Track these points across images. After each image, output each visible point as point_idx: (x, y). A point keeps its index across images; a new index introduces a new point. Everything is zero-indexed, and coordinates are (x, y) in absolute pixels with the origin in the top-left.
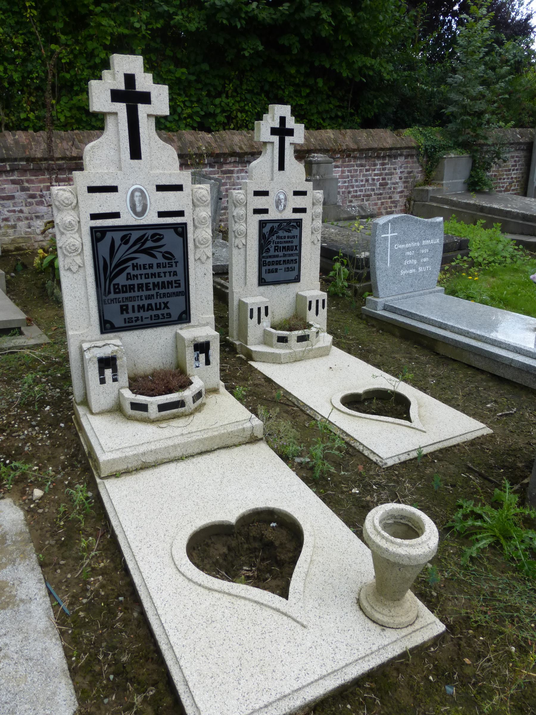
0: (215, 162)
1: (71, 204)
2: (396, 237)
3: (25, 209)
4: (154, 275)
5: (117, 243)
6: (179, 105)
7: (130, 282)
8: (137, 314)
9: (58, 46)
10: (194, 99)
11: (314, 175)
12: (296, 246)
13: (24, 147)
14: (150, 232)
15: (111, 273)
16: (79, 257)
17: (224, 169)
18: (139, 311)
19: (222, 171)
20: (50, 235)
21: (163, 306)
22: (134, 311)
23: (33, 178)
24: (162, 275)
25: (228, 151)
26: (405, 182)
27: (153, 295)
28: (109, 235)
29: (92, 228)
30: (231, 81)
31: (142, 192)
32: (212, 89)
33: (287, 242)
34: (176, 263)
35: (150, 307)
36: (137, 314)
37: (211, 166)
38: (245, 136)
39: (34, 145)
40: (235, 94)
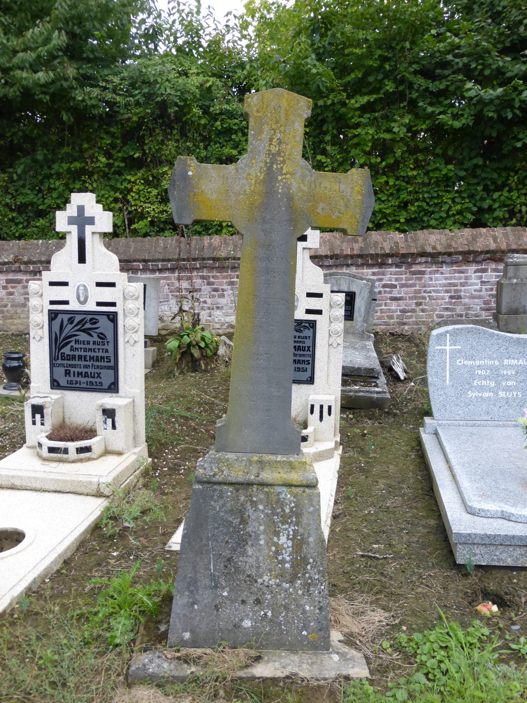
0: (401, 262)
1: (37, 293)
2: (459, 351)
3: (209, 301)
4: (90, 350)
5: (65, 323)
6: (446, 202)
7: (72, 353)
8: (76, 378)
9: (324, 157)
10: (465, 195)
11: (510, 278)
12: (309, 347)
13: (215, 249)
14: (89, 317)
15: (60, 344)
16: (41, 330)
17: (413, 269)
18: (78, 377)
19: (410, 272)
20: (226, 324)
21: (96, 375)
22: (74, 376)
23: (219, 274)
24: (97, 350)
25: (415, 251)
27: (89, 366)
28: (60, 316)
29: (49, 311)
30: (516, 173)
31: (85, 286)
32: (489, 183)
33: (298, 342)
34: (108, 342)
35: (86, 375)
36: (76, 378)
37: (397, 266)
38: (446, 235)
39: (224, 247)
40: (520, 186)
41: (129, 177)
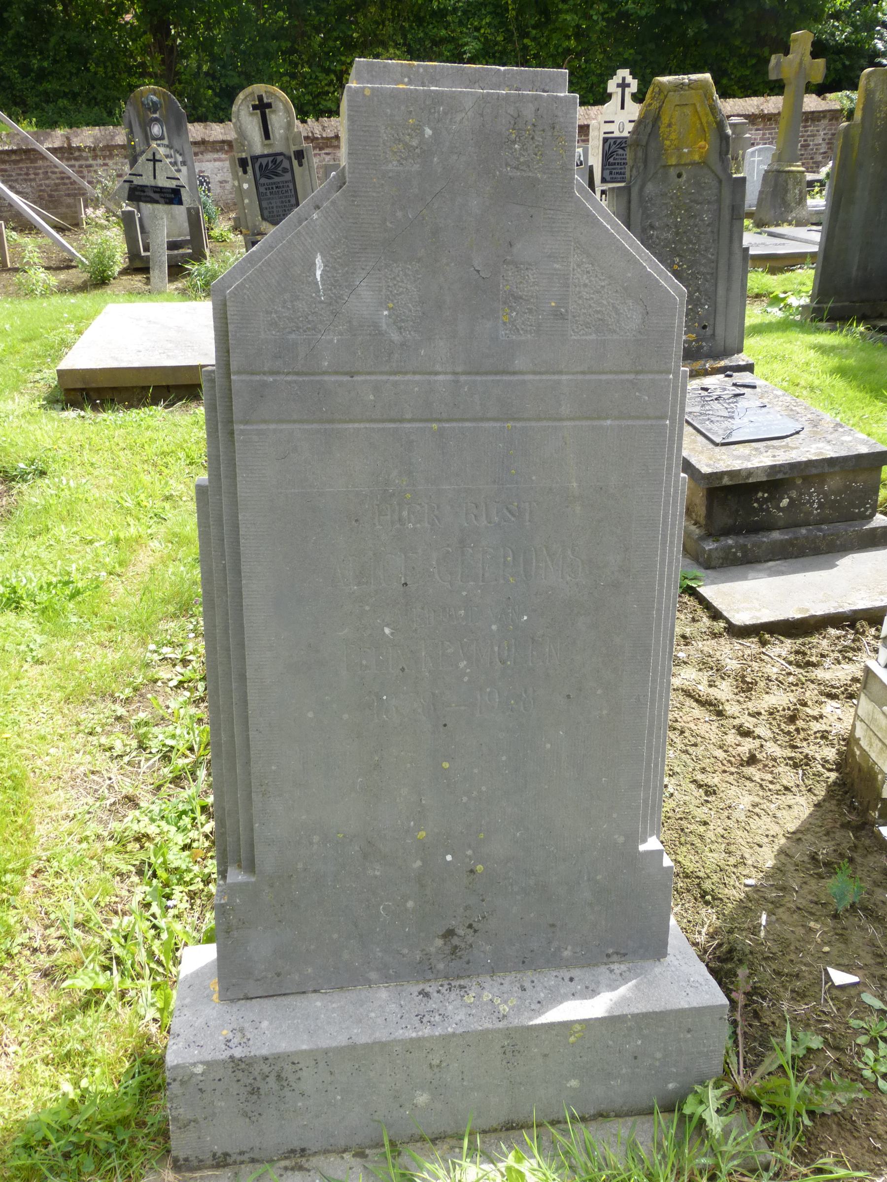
26: (828, 144)
41: (343, 58)
